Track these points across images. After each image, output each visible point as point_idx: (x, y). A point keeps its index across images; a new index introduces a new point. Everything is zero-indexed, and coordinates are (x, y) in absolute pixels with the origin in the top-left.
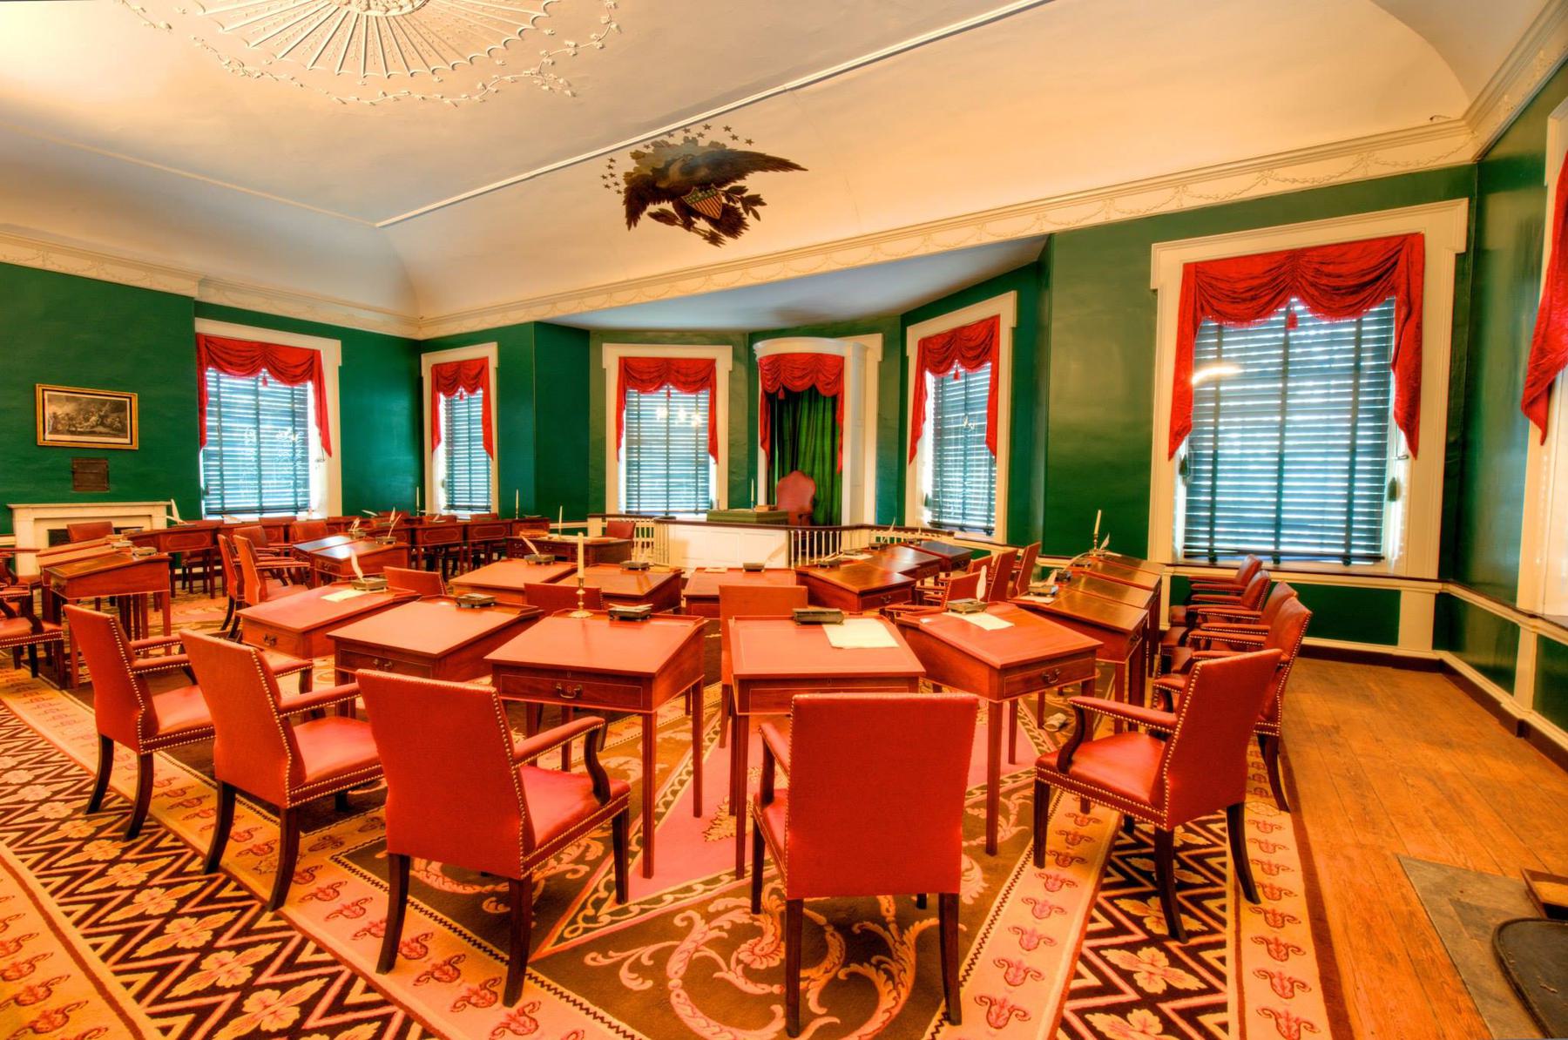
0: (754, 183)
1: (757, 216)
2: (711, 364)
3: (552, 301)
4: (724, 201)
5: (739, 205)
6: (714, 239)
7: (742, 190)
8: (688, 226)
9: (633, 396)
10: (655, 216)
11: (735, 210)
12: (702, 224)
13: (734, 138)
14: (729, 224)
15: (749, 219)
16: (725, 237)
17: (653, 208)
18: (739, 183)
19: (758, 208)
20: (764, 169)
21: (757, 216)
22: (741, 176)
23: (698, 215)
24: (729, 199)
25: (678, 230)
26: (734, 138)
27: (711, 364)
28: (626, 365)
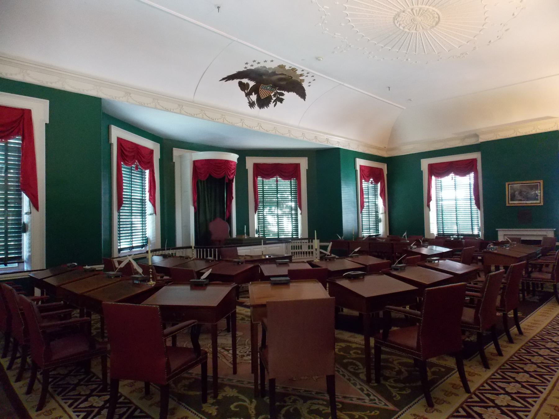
0: (290, 97)
3: (128, 91)
4: (272, 95)
5: (274, 99)
6: (252, 105)
7: (283, 94)
8: (248, 95)
11: (272, 99)
12: (254, 97)
14: (263, 103)
15: (272, 105)
16: (256, 106)
17: (245, 81)
18: (285, 93)
19: (278, 103)
21: (275, 105)
22: (288, 91)
23: (257, 92)
24: (274, 95)
25: (243, 93)
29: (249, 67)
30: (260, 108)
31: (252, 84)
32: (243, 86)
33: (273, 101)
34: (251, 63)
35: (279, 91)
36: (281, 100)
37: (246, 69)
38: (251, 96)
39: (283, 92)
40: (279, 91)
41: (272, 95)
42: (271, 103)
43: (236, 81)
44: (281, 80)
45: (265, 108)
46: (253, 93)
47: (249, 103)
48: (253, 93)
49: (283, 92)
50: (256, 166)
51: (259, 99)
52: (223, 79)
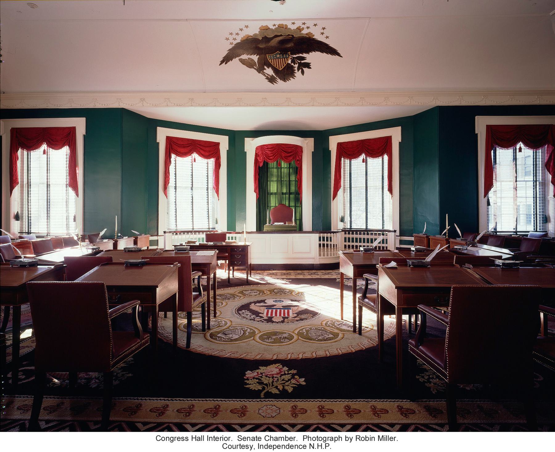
0: (312, 57)
1: (303, 73)
2: (218, 144)
4: (290, 62)
5: (296, 66)
6: (271, 80)
7: (304, 58)
8: (260, 70)
9: (345, 162)
10: (243, 62)
11: (293, 67)
12: (269, 71)
13: (327, 37)
14: (286, 73)
15: (298, 74)
16: (279, 80)
17: (245, 57)
18: (304, 55)
19: (305, 70)
20: (327, 53)
21: (303, 73)
22: (308, 52)
23: (269, 65)
24: (293, 61)
25: (253, 71)
26: (327, 37)
27: (218, 144)
28: (169, 140)
29: (235, 42)
30: (285, 81)
31: (255, 58)
32: (249, 64)
33: (296, 69)
34: (231, 38)
35: (295, 56)
36: (308, 65)
37: (233, 45)
38: (265, 71)
39: (301, 55)
40: (295, 56)
41: (290, 62)
42: (296, 71)
43: (236, 61)
44: (282, 42)
45: (291, 79)
46: (265, 67)
47: (267, 78)
48: (265, 67)
49: (301, 55)
50: (340, 145)
51: (275, 70)
52: (222, 62)
